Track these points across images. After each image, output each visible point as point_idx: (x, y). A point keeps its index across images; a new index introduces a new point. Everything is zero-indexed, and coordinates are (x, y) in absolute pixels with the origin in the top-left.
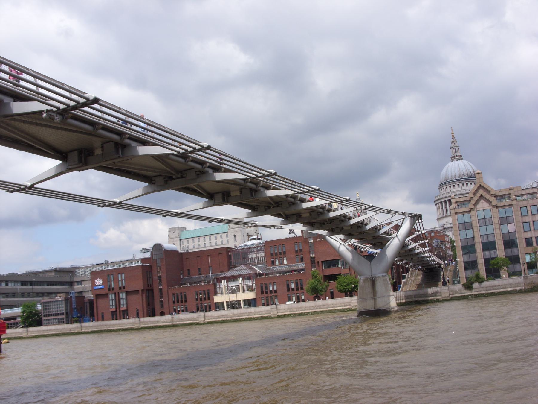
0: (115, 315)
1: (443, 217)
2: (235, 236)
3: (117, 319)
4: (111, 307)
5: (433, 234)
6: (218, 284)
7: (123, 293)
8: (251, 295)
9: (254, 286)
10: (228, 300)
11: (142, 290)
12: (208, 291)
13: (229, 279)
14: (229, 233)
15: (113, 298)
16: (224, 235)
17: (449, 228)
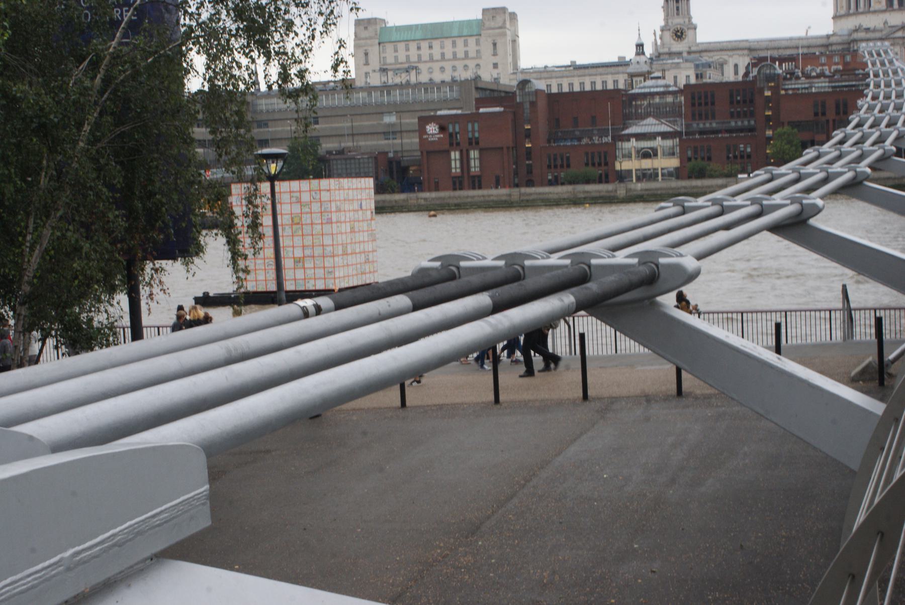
0: (458, 183)
1: (848, 15)
2: (495, 45)
3: (461, 189)
4: (453, 171)
5: (848, 58)
6: (620, 143)
7: (474, 149)
8: (673, 163)
9: (677, 150)
10: (638, 167)
11: (508, 148)
12: (606, 153)
13: (640, 137)
14: (482, 39)
15: (458, 156)
16: (472, 41)
17: (862, 40)
